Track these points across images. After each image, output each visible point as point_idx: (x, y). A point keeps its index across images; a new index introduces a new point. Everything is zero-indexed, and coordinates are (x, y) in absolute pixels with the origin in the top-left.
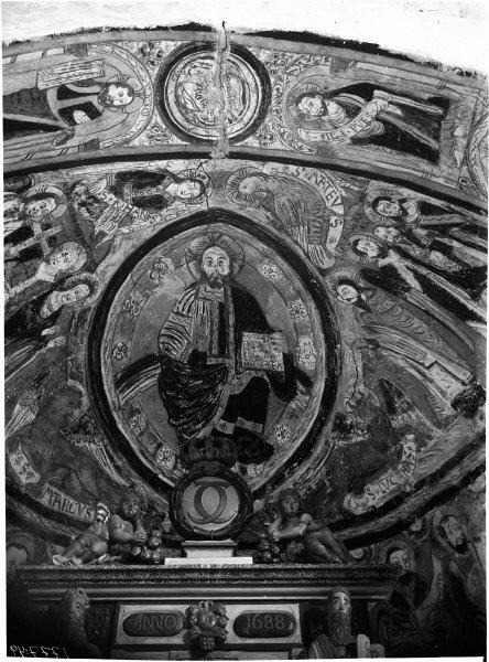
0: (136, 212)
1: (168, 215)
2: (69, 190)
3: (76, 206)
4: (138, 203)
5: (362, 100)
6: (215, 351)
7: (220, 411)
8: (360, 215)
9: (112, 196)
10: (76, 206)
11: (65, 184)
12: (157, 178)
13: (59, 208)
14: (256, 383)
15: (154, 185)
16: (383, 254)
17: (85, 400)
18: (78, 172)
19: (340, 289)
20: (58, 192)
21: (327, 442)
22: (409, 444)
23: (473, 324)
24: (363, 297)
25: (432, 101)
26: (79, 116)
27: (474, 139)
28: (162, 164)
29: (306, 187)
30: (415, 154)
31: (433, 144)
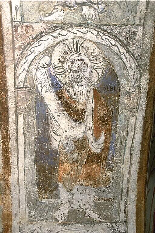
27: (84, 30)
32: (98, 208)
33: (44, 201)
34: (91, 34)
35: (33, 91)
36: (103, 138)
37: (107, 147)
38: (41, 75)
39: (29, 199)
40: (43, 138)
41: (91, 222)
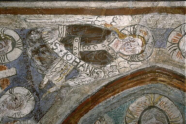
0: (82, 66)
2: (26, 35)
3: (30, 53)
4: (85, 57)
9: (63, 48)
10: (30, 53)
11: (23, 29)
12: (102, 34)
13: (13, 52)
15: (100, 40)
20: (16, 37)
28: (108, 19)
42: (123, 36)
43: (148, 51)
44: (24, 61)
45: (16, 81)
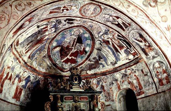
1: (72, 25)
2: (57, 21)
4: (68, 23)
5: (117, 19)
6: (71, 46)
7: (69, 55)
8: (107, 32)
9: (64, 22)
12: (74, 20)
14: (77, 52)
16: (108, 39)
17: (47, 52)
18: (60, 18)
19: (98, 41)
21: (87, 63)
22: (101, 66)
23: (119, 53)
24: (102, 43)
25: (128, 23)
26: (65, 10)
29: (100, 26)
30: (121, 28)
31: (125, 29)
32: (156, 54)
33: (148, 57)
34: (133, 31)
35: (134, 42)
36: (147, 43)
37: (149, 44)
38: (133, 39)
39: (146, 58)
40: (141, 47)
41: (156, 57)
42: (77, 21)
43: (81, 23)
44: (56, 24)
45: (53, 27)
